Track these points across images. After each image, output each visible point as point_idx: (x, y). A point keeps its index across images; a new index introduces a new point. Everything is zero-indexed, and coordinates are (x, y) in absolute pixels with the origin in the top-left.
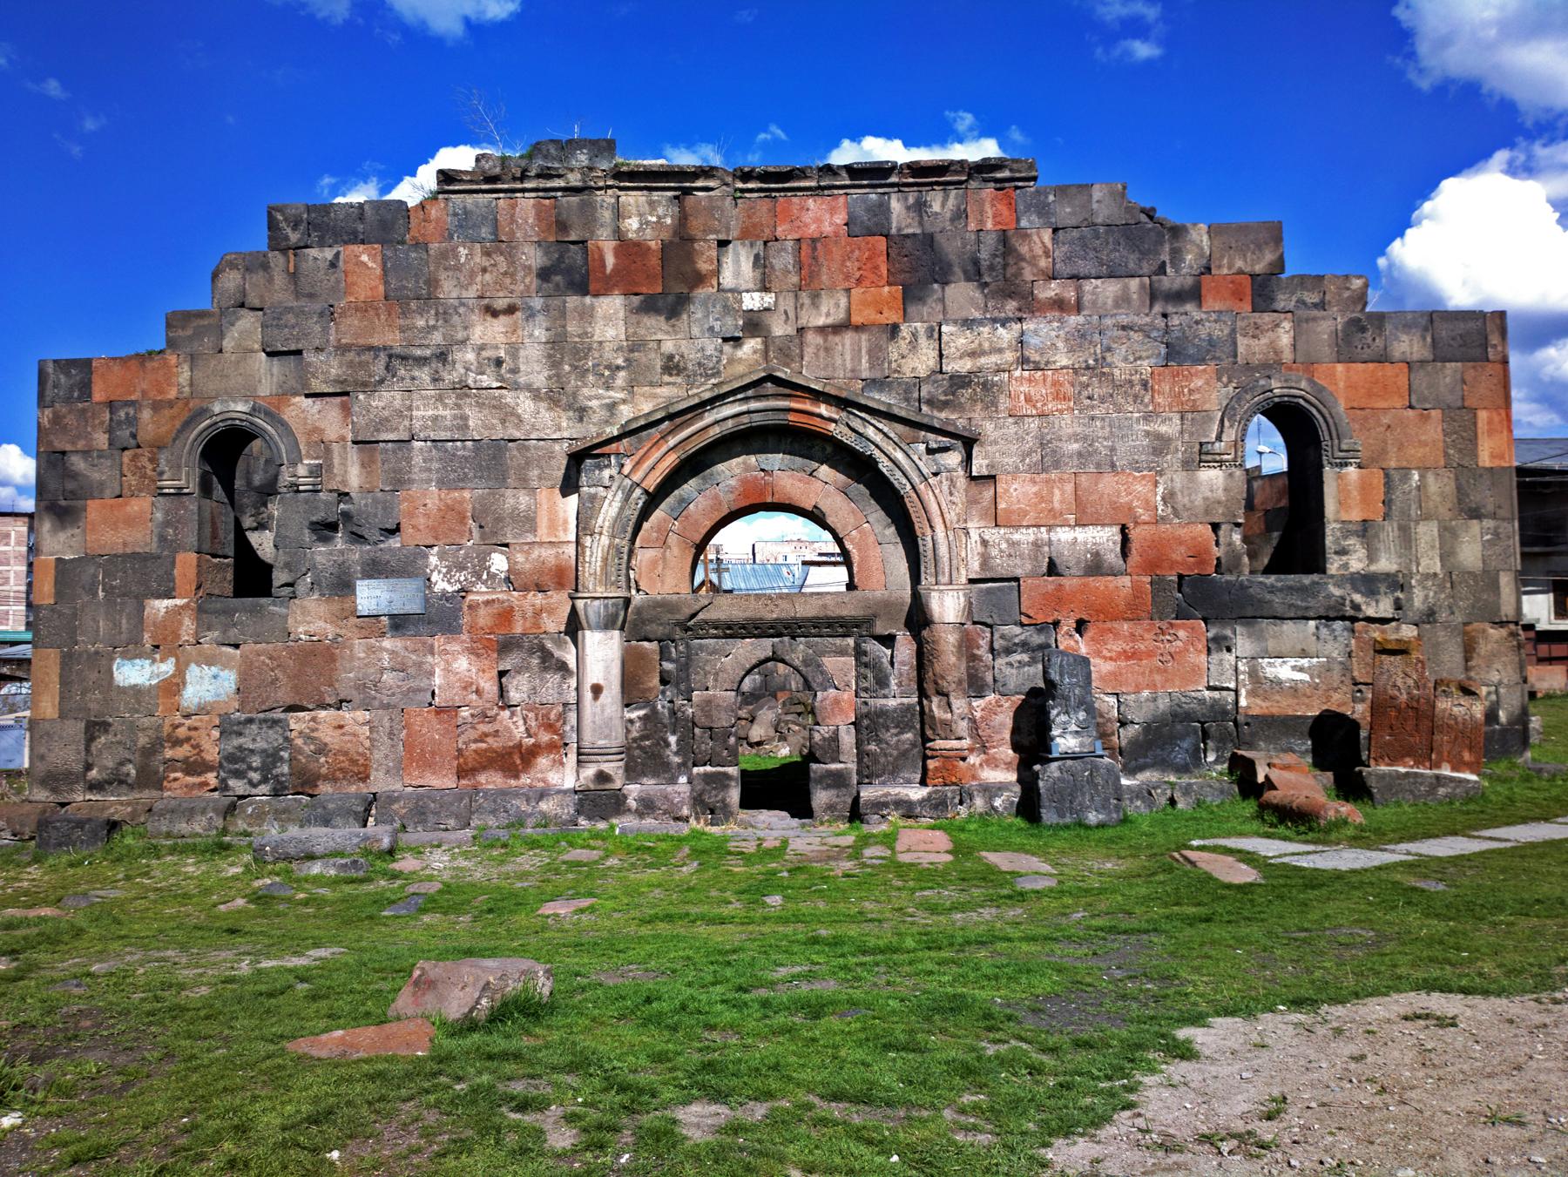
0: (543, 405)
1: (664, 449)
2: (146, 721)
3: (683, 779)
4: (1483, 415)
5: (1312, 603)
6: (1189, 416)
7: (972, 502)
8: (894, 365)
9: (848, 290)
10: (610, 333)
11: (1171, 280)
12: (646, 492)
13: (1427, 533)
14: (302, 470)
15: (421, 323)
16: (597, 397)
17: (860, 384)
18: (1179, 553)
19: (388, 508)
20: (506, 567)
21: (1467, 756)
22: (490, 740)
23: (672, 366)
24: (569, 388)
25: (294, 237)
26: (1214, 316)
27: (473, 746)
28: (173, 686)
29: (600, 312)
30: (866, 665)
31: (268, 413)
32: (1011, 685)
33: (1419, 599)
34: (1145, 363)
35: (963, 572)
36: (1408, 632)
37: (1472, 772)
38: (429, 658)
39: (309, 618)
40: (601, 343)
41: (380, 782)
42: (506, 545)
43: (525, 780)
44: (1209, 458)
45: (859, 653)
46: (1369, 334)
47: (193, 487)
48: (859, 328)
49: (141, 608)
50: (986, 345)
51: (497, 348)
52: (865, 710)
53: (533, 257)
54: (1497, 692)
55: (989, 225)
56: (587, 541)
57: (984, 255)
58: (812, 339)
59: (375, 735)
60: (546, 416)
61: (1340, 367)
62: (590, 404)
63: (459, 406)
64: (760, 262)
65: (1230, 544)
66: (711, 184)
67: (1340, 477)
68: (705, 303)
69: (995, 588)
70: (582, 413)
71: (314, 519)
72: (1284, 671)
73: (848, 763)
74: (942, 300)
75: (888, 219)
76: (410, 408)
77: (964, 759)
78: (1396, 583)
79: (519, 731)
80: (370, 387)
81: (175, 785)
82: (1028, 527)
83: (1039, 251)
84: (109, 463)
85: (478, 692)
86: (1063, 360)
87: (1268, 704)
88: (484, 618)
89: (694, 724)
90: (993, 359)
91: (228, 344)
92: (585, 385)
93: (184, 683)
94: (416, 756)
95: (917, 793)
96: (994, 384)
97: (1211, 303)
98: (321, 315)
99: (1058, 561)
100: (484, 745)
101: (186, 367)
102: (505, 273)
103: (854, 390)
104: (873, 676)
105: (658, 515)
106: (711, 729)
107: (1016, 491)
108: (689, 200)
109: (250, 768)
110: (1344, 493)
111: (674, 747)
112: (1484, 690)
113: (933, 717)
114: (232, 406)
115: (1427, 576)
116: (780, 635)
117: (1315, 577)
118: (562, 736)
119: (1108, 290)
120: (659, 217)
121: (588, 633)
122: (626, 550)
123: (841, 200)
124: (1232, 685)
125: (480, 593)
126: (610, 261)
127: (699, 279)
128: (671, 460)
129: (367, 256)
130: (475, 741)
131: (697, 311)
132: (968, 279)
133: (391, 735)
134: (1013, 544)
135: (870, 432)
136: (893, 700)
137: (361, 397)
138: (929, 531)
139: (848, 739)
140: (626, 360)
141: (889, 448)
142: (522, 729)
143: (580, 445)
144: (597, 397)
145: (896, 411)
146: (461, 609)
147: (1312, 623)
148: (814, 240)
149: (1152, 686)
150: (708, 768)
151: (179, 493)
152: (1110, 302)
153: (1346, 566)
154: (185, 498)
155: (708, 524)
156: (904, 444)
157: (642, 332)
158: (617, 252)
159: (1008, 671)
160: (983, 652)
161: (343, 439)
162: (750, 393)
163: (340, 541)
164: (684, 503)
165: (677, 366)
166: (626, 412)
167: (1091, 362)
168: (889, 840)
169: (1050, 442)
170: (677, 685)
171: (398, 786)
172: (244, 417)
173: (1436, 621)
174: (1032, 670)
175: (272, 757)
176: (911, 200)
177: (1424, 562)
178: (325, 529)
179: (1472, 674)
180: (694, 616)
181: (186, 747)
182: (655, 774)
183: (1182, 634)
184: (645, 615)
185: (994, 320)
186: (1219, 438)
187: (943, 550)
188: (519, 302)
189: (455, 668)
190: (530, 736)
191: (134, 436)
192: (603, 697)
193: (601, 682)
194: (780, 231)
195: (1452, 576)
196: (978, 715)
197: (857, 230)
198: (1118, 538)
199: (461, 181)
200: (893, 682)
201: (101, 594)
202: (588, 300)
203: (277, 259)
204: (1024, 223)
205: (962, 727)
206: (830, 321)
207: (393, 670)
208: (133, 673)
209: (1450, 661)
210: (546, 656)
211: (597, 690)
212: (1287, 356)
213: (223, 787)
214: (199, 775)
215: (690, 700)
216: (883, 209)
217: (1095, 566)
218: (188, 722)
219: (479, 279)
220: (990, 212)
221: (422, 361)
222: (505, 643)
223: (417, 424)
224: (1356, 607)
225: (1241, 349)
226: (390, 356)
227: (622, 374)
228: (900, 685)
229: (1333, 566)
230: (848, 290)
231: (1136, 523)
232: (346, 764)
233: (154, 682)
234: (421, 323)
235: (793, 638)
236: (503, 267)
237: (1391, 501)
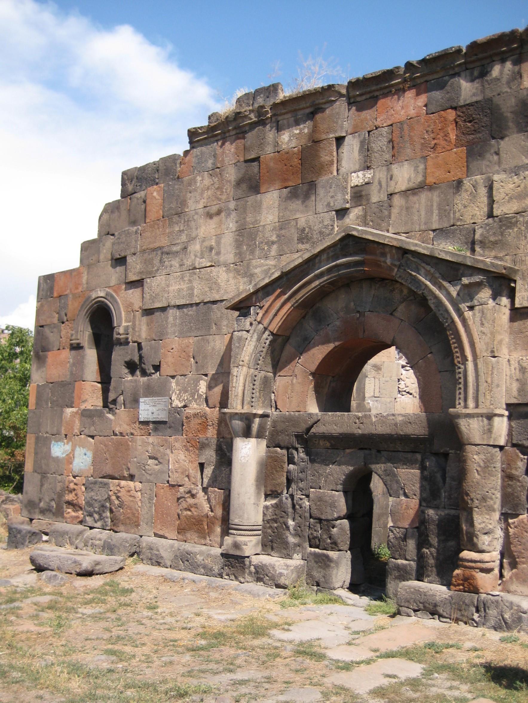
0: (231, 275)
8: (458, 215)
9: (425, 158)
12: (272, 333)
16: (261, 266)
23: (304, 237)
25: (130, 188)
28: (70, 459)
29: (265, 205)
40: (264, 226)
48: (431, 188)
49: (62, 412)
53: (231, 174)
58: (397, 201)
60: (232, 281)
64: (366, 150)
68: (324, 187)
71: (126, 360)
74: (497, 153)
76: (168, 286)
85: (188, 476)
100: (189, 513)
116: (370, 449)
130: (186, 509)
131: (321, 191)
137: (148, 280)
140: (278, 236)
180: (309, 429)
184: (279, 428)
197: (432, 108)
206: (411, 185)
226: (162, 253)
227: (275, 247)
228: (449, 498)
230: (425, 158)
233: (64, 455)
234: (177, 229)
235: (379, 451)
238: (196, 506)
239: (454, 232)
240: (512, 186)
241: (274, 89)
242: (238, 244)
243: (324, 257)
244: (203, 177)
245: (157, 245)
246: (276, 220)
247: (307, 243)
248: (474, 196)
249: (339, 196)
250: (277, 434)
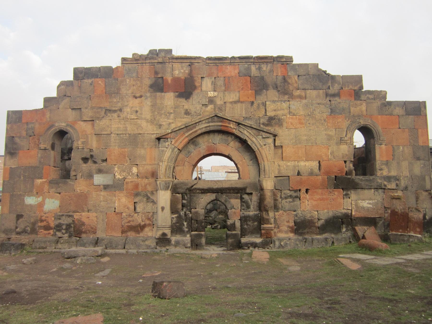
0: (149, 124)
1: (184, 137)
2: (34, 215)
3: (188, 236)
4: (420, 131)
5: (373, 184)
6: (338, 129)
7: (275, 154)
10: (169, 103)
12: (179, 149)
13: (405, 164)
14: (80, 143)
15: (115, 100)
16: (165, 121)
17: (242, 119)
18: (335, 170)
20: (137, 171)
21: (418, 230)
22: (131, 222)
23: (187, 113)
24: (157, 119)
26: (344, 101)
27: (126, 224)
28: (41, 205)
30: (244, 202)
31: (71, 126)
32: (287, 208)
33: (403, 183)
34: (325, 114)
35: (273, 174)
36: (399, 193)
37: (420, 234)
38: (114, 198)
39: (80, 186)
40: (166, 106)
41: (100, 234)
42: (137, 165)
43: (141, 234)
44: (343, 142)
45: (242, 198)
46: (387, 107)
47: (49, 147)
48: (242, 102)
49: (33, 182)
50: (279, 108)
51: (136, 107)
52: (243, 215)
53: (148, 82)
54: (425, 211)
55: (280, 74)
56: (161, 164)
57: (279, 83)
58: (228, 105)
59: (98, 220)
61: (379, 117)
62: (162, 123)
63: (125, 124)
64: (214, 84)
65: (349, 167)
66: (199, 61)
67: (380, 148)
69: (282, 179)
70: (160, 126)
71: (83, 157)
72: (365, 204)
73: (238, 232)
74: (266, 95)
75: (251, 72)
76: (111, 125)
77: (272, 230)
78: (397, 179)
79: (140, 221)
80: (99, 119)
81: (41, 233)
82: (292, 161)
83: (294, 81)
84: (26, 140)
85: (128, 208)
86: (302, 113)
87: (360, 214)
88: (130, 186)
89: (192, 219)
91: (61, 106)
92: (162, 118)
93: (45, 204)
95: (258, 240)
96: (281, 119)
98: (87, 98)
99: (300, 172)
101: (49, 113)
102: (140, 86)
103: (241, 120)
104: (245, 205)
106: (197, 221)
107: (288, 151)
108: (193, 66)
109: (62, 229)
110: (381, 153)
111: (186, 226)
112: (422, 210)
113: (264, 218)
114: (61, 124)
115: (405, 177)
116: (218, 193)
117: (373, 177)
118: (152, 222)
119: (314, 93)
120: (184, 71)
121: (160, 191)
122: (172, 167)
123: (237, 66)
124: (350, 208)
125: (129, 179)
126: (170, 81)
127: (195, 88)
128: (187, 140)
130: (127, 223)
132: (274, 89)
133: (103, 220)
134: (287, 166)
135: (245, 132)
136: (252, 212)
137: (97, 121)
138: (263, 162)
139: (238, 224)
140: (174, 111)
141: (251, 137)
142: (141, 220)
143: (158, 136)
144: (165, 121)
145: (253, 126)
146: (124, 184)
147: (373, 190)
148: (229, 77)
150: (196, 233)
151: (45, 149)
152: (314, 97)
153: (382, 174)
154: (47, 150)
155: (197, 159)
157: (178, 103)
158: (172, 80)
159: (286, 204)
160: (279, 198)
161: (92, 134)
162: (210, 120)
163: (90, 162)
165: (188, 113)
166: (173, 126)
167: (309, 113)
168: (250, 255)
169: (298, 136)
170: (187, 207)
171: (105, 236)
172: (64, 127)
173: (407, 190)
174: (292, 204)
175: (69, 226)
176: (257, 67)
177: (404, 173)
178: (85, 160)
179: (418, 205)
180: (193, 186)
181: (45, 222)
182: (180, 234)
183: (336, 193)
184: (178, 186)
185: (282, 101)
186: (346, 136)
187: (267, 168)
188: (143, 94)
189: (122, 201)
190: (143, 222)
191: (33, 132)
192: (164, 211)
193: (164, 206)
194: (219, 75)
195: (412, 177)
196: (277, 217)
197: (241, 74)
198: (318, 165)
199: (128, 61)
200: (252, 207)
201: (22, 178)
202: (163, 94)
203: (76, 83)
204: (289, 74)
205: (272, 220)
206: (234, 100)
207: (104, 201)
208: (31, 201)
209: (412, 201)
210: (148, 198)
211: (163, 209)
212: (365, 113)
213: (55, 235)
214: (49, 230)
215: (191, 212)
216: (249, 69)
217: (311, 173)
218: (45, 215)
219: (132, 88)
220: (279, 70)
221: (115, 111)
222: (136, 193)
223: (113, 129)
224: (385, 186)
225: (352, 111)
226: (106, 110)
227: (172, 115)
228: (254, 208)
229: (379, 173)
231: (323, 160)
232: (90, 229)
233: (36, 203)
234: (115, 100)
235: (222, 193)
236: (139, 84)
237: (394, 155)
238: (133, 221)
239: (251, 119)
240: (273, 107)
241: (170, 51)
243: (204, 122)
244: (130, 80)
245: (102, 106)
246: (173, 104)
247: (189, 115)
248: (258, 107)
249: (204, 100)
250: (177, 188)
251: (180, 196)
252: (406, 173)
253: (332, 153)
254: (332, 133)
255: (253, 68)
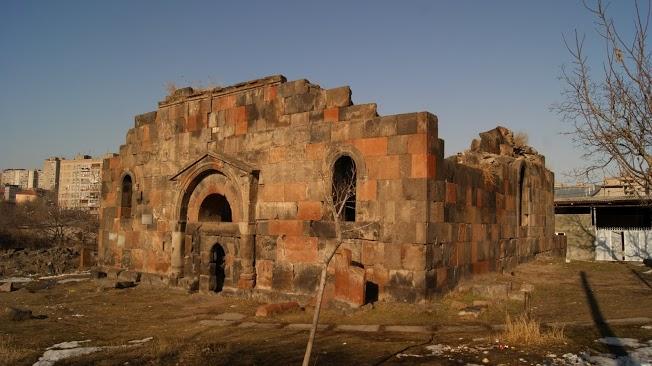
4: (414, 156)
11: (315, 113)
13: (391, 206)
19: (147, 194)
28: (116, 240)
33: (386, 233)
39: (135, 225)
41: (144, 270)
53: (173, 123)
61: (364, 140)
64: (217, 119)
73: (231, 278)
78: (377, 226)
80: (146, 163)
90: (265, 144)
94: (149, 264)
95: (235, 290)
97: (327, 120)
105: (192, 196)
110: (363, 190)
119: (297, 117)
125: (162, 220)
127: (203, 125)
129: (146, 128)
134: (268, 208)
139: (231, 270)
149: (302, 260)
156: (237, 174)
164: (198, 193)
177: (388, 217)
178: (140, 200)
189: (156, 240)
212: (346, 138)
216: (244, 98)
217: (288, 217)
229: (357, 218)
242: (176, 153)
251: (190, 237)
252: (391, 217)
253: (309, 192)
254: (309, 166)
255: (248, 96)
